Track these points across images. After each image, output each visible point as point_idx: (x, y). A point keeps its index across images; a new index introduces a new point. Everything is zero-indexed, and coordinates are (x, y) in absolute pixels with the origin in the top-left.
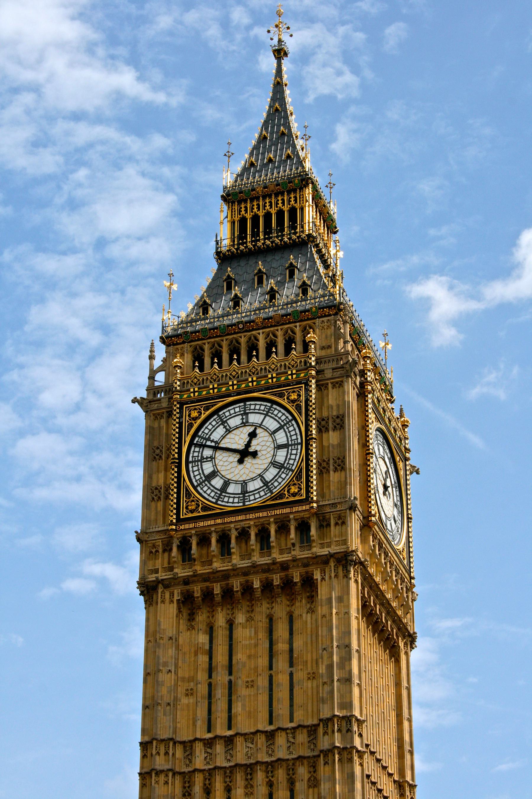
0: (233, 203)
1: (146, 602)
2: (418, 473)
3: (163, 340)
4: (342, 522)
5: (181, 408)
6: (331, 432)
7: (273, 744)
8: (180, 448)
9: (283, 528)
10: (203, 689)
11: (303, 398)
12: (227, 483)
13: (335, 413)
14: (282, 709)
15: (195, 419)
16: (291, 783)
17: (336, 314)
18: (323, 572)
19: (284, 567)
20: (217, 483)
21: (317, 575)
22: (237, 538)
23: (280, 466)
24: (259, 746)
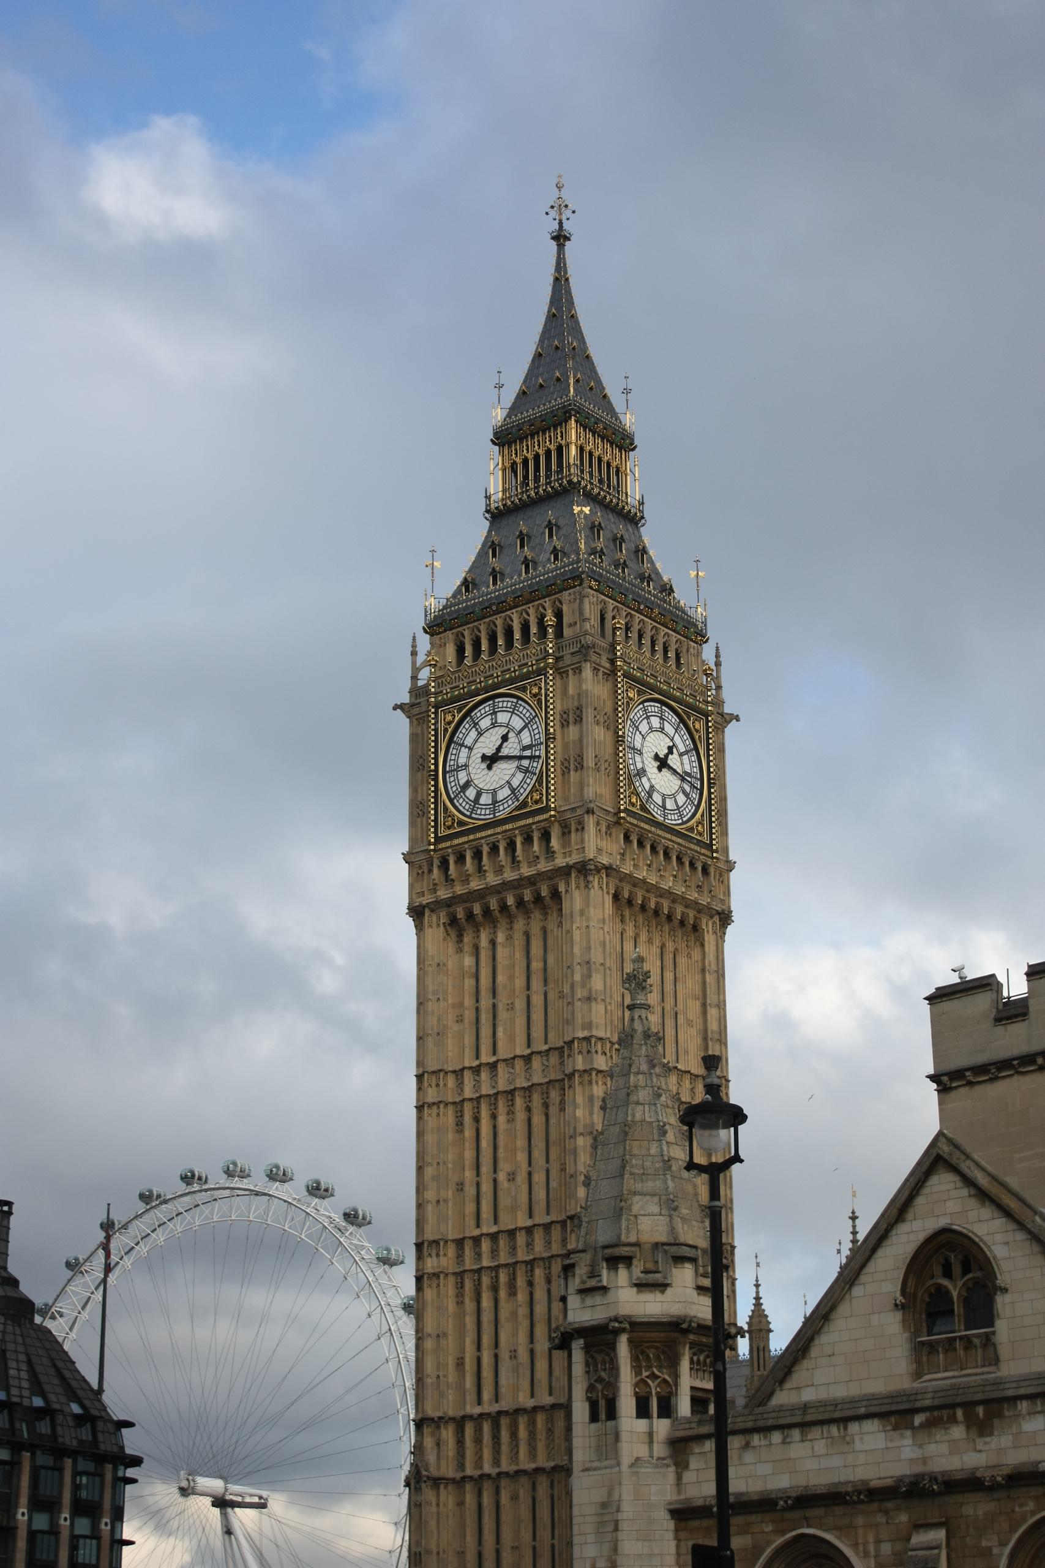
0: (503, 446)
1: (416, 927)
2: (738, 720)
3: (426, 632)
4: (581, 827)
5: (436, 713)
6: (571, 727)
7: (530, 1068)
8: (436, 759)
9: (528, 840)
10: (469, 1015)
11: (543, 691)
12: (479, 795)
13: (576, 704)
14: (537, 1032)
15: (450, 723)
16: (546, 1105)
17: (581, 584)
19: (532, 881)
20: (471, 793)
21: (562, 888)
22: (489, 853)
23: (526, 771)
24: (518, 1071)
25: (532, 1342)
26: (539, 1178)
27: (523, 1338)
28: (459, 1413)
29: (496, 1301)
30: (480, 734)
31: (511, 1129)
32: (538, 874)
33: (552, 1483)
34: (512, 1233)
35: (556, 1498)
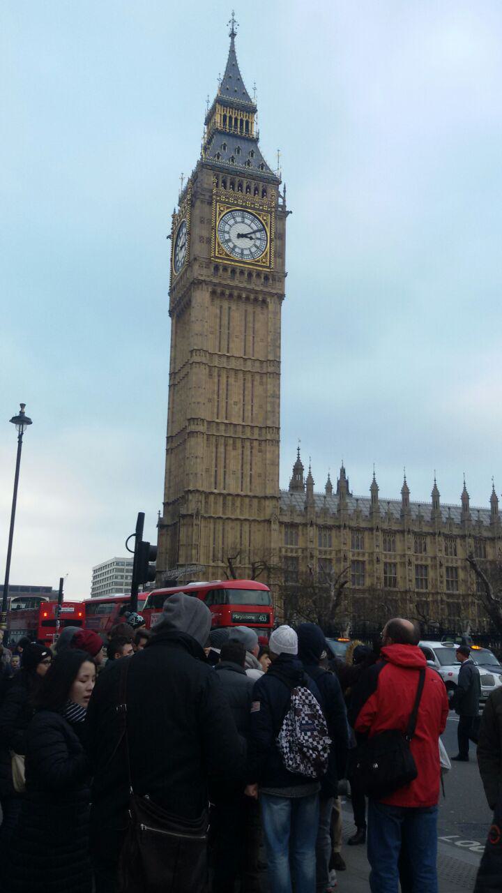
14: (250, 350)
16: (253, 381)
18: (271, 300)
19: (257, 292)
20: (231, 245)
21: (268, 300)
25: (242, 470)
26: (250, 407)
27: (240, 468)
28: (208, 491)
29: (225, 449)
30: (236, 222)
31: (236, 386)
32: (262, 291)
33: (250, 525)
34: (235, 425)
35: (252, 531)
